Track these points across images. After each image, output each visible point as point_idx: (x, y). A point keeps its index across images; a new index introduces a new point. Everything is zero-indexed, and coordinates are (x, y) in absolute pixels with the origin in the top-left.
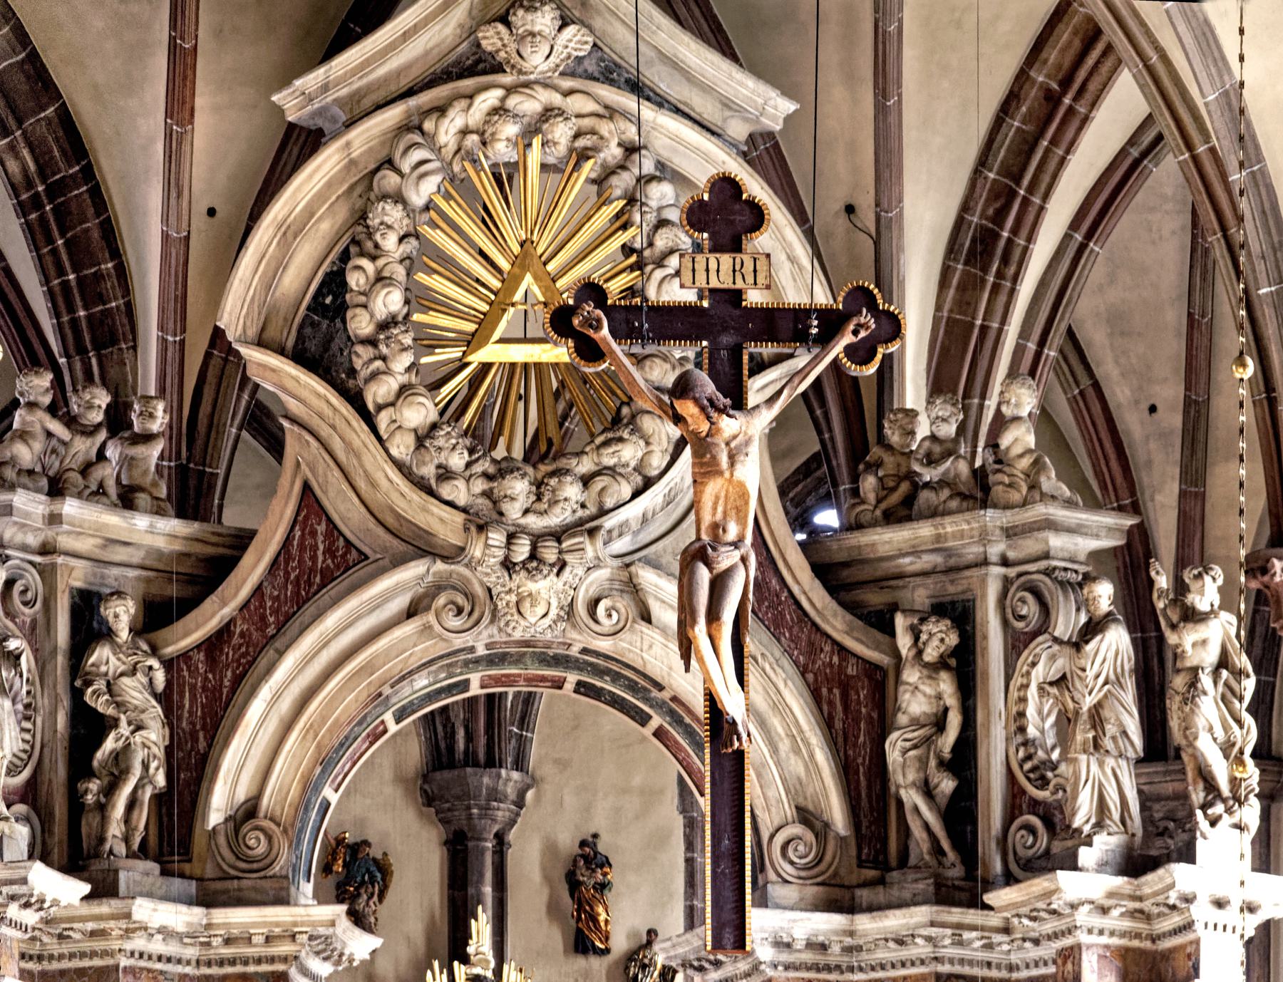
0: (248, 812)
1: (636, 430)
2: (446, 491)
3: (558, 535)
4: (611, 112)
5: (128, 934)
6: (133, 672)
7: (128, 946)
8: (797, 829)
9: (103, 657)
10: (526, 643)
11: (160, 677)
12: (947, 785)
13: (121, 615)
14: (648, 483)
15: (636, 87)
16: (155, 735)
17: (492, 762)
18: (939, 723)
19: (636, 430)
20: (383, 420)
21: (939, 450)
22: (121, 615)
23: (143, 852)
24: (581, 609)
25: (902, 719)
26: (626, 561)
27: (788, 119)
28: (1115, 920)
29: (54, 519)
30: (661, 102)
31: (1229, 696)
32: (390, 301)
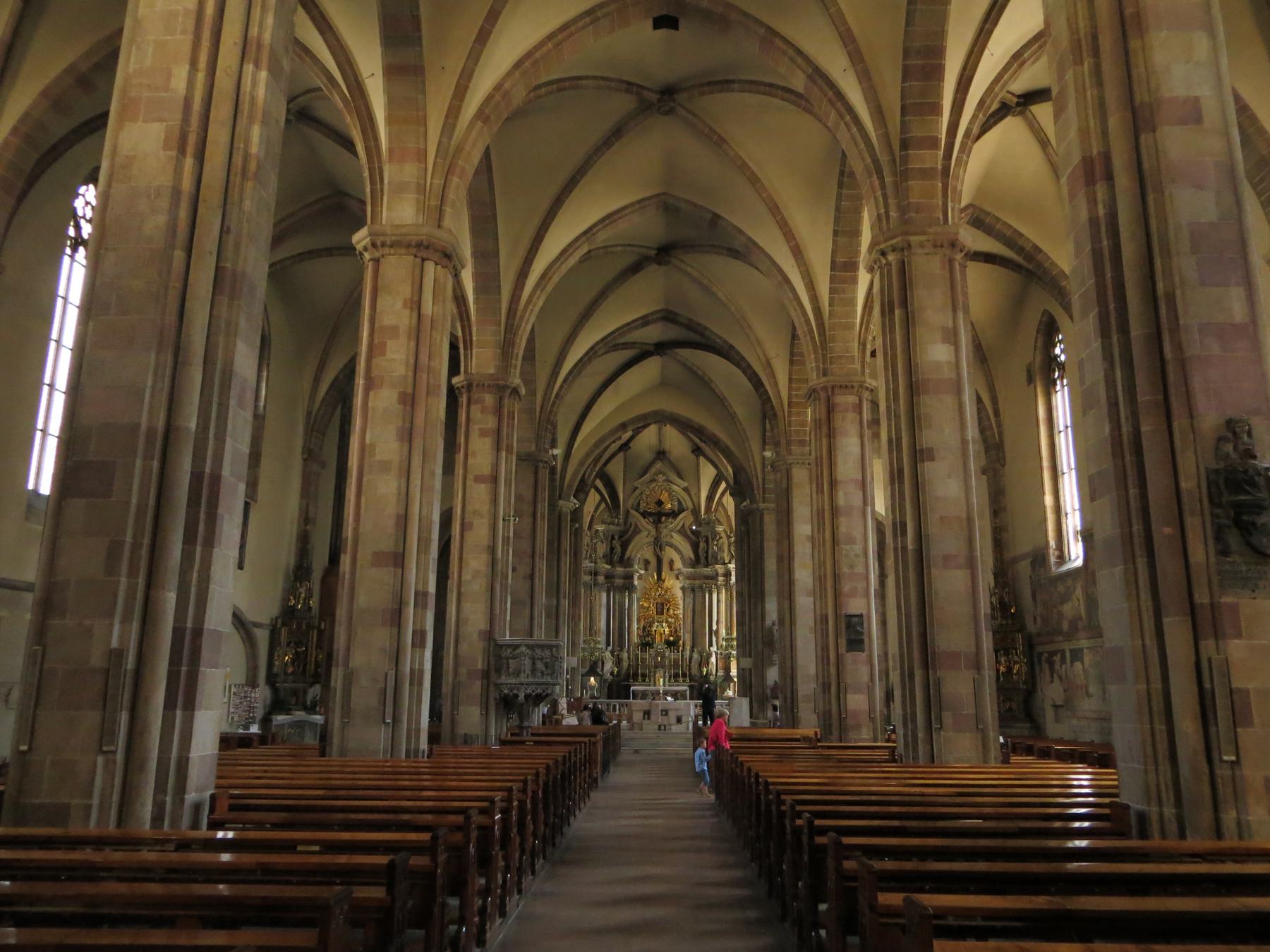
0: (629, 558)
9: (614, 542)
13: (616, 537)
22: (616, 537)
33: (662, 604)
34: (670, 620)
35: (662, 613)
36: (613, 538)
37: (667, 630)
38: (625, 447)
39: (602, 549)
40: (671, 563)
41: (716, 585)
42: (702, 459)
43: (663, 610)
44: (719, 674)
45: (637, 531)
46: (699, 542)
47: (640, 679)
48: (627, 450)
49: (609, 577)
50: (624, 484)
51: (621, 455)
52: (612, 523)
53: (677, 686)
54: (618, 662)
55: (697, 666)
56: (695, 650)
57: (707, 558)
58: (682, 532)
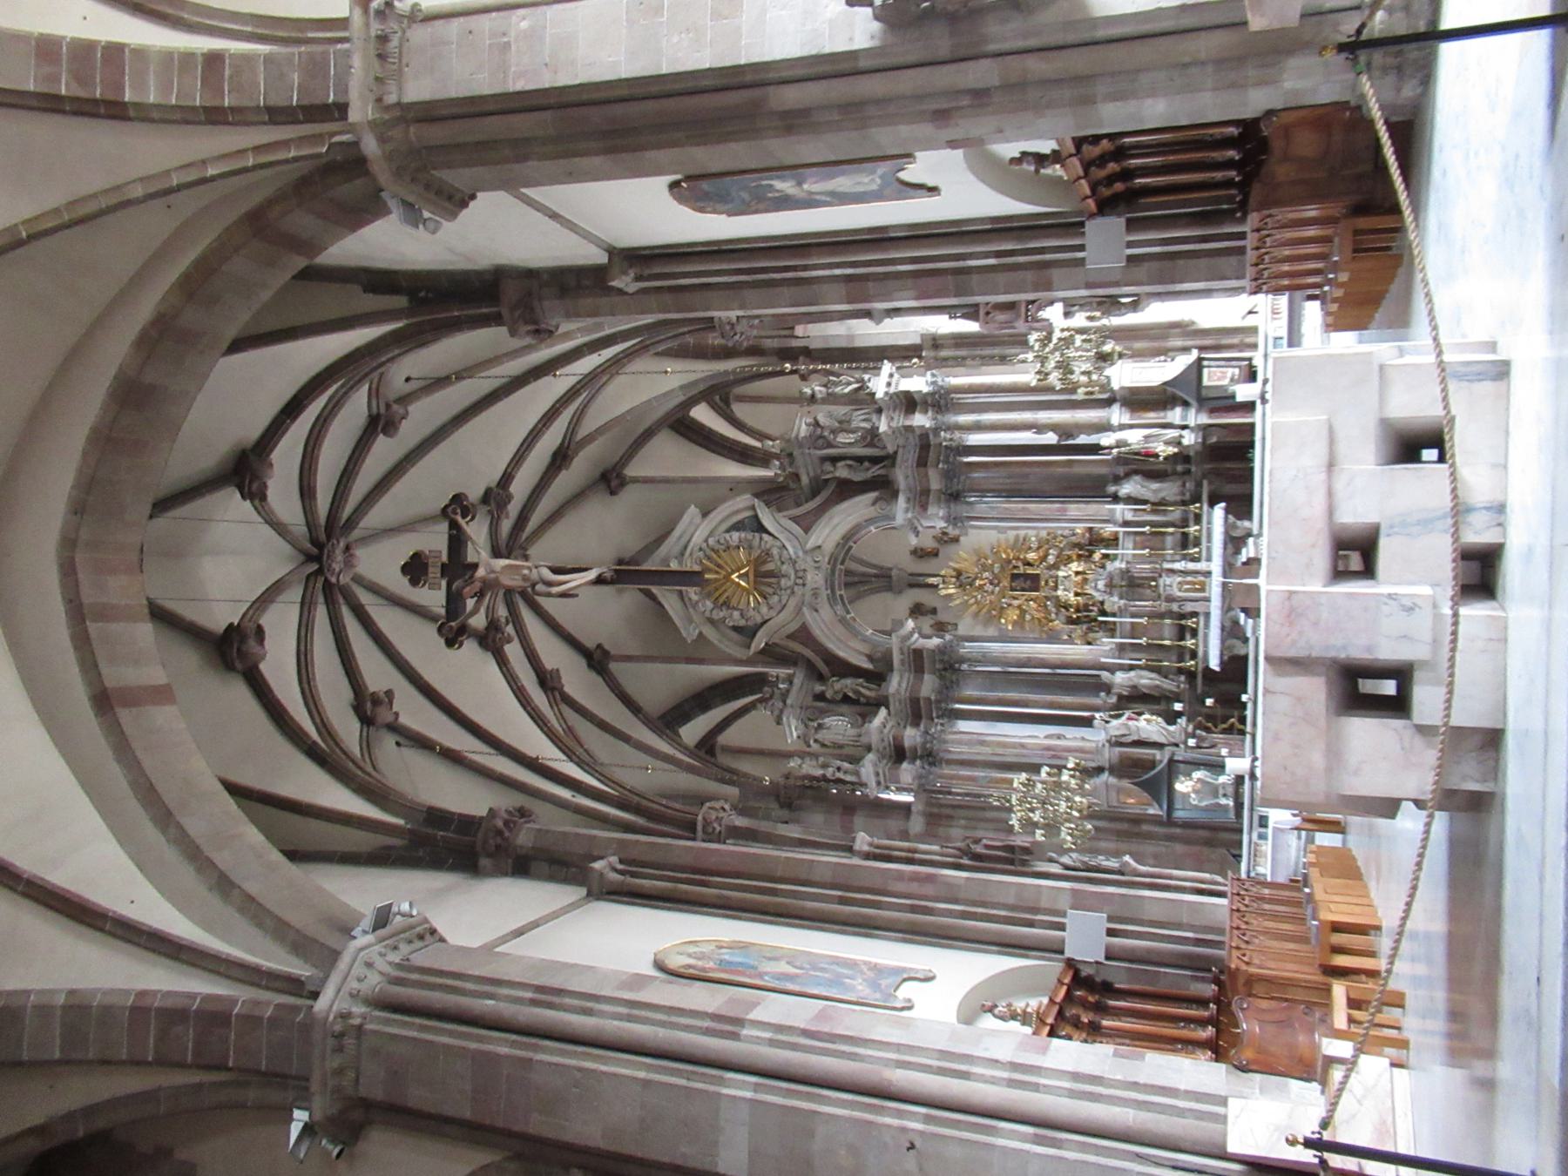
0: (870, 658)
1: (769, 550)
2: (784, 602)
3: (796, 571)
4: (691, 554)
5: (899, 693)
6: (832, 686)
7: (903, 693)
8: (877, 506)
9: (829, 695)
10: (826, 581)
11: (834, 679)
12: (866, 464)
13: (819, 688)
14: (784, 546)
15: (686, 547)
16: (849, 681)
17: (890, 577)
18: (850, 466)
19: (769, 550)
20: (766, 618)
21: (782, 467)
22: (819, 688)
23: (880, 686)
24: (816, 565)
25: (849, 477)
26: (806, 552)
27: (696, 506)
28: (896, 417)
29: (792, 706)
30: (689, 541)
31: (836, 384)
32: (736, 614)
33: (1014, 577)
34: (1051, 560)
35: (1036, 578)
36: (820, 697)
37: (1075, 566)
38: (597, 660)
39: (838, 726)
40: (920, 554)
41: (936, 430)
42: (631, 471)
43: (1026, 576)
44: (1177, 421)
45: (803, 634)
46: (836, 478)
47: (1189, 643)
48: (606, 653)
49: (916, 712)
50: (701, 661)
51: (614, 667)
52: (784, 696)
53: (1209, 540)
54: (1136, 699)
55: (1155, 486)
56: (1112, 489)
57: (875, 460)
58: (807, 523)
